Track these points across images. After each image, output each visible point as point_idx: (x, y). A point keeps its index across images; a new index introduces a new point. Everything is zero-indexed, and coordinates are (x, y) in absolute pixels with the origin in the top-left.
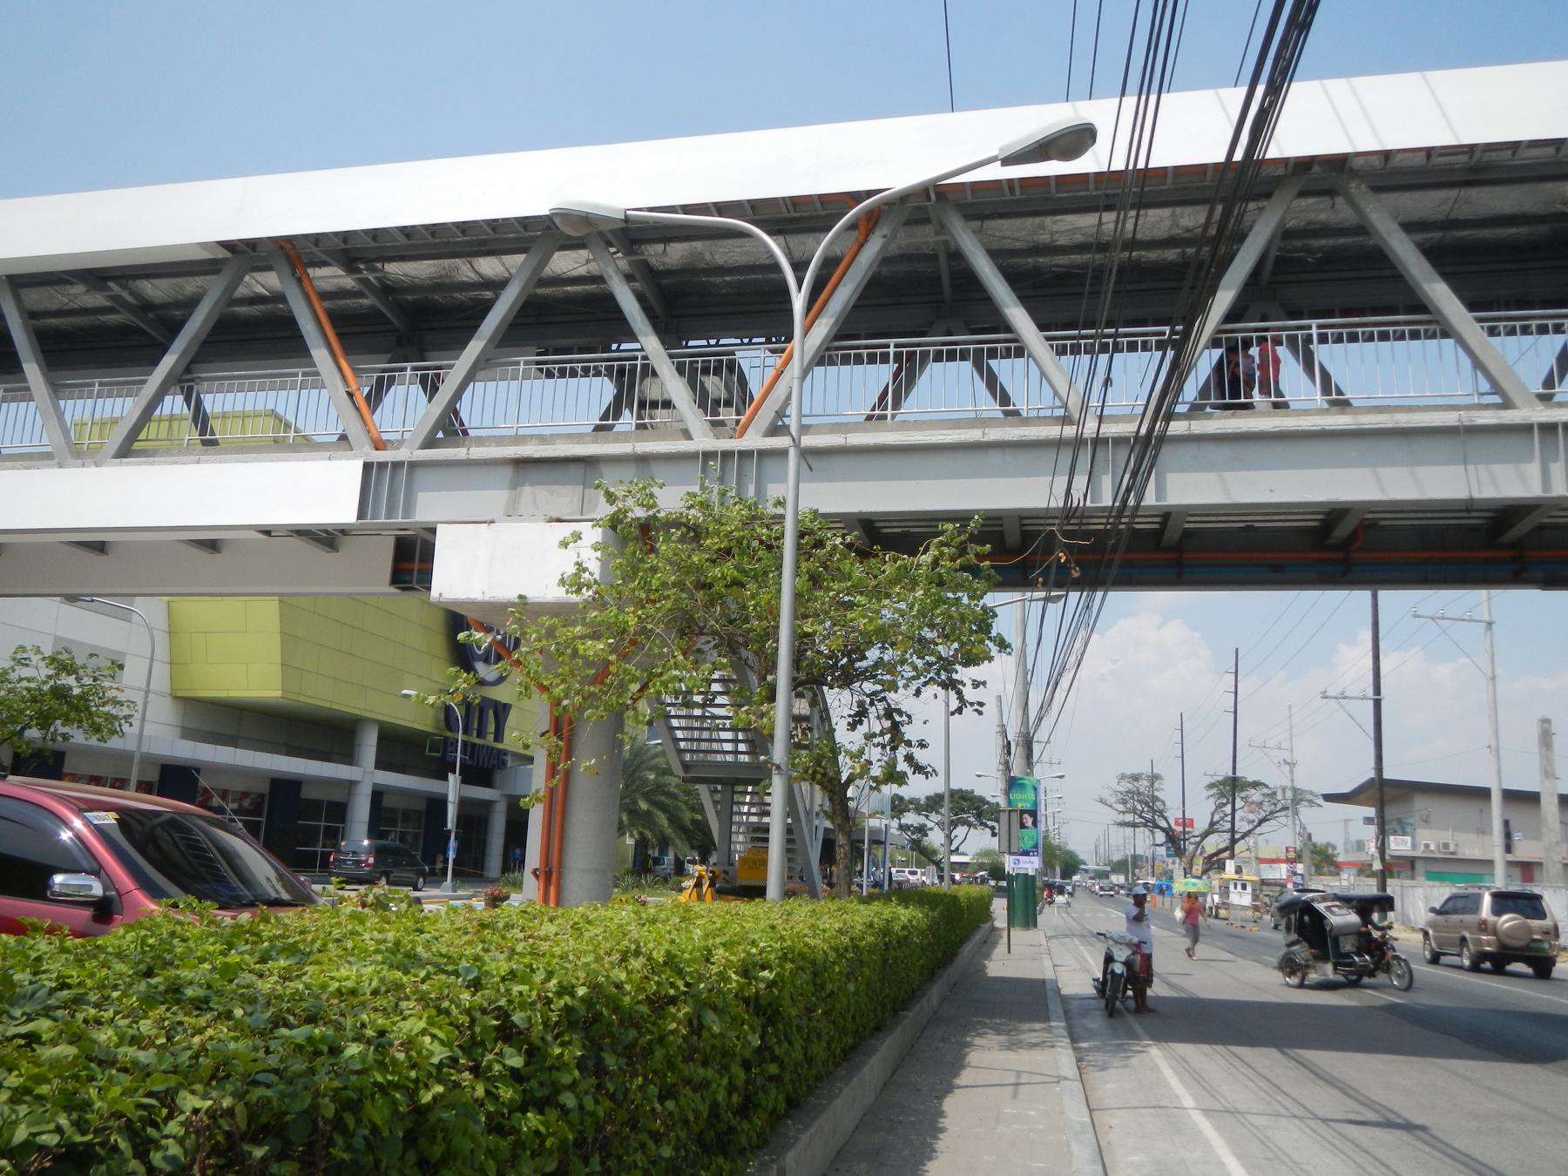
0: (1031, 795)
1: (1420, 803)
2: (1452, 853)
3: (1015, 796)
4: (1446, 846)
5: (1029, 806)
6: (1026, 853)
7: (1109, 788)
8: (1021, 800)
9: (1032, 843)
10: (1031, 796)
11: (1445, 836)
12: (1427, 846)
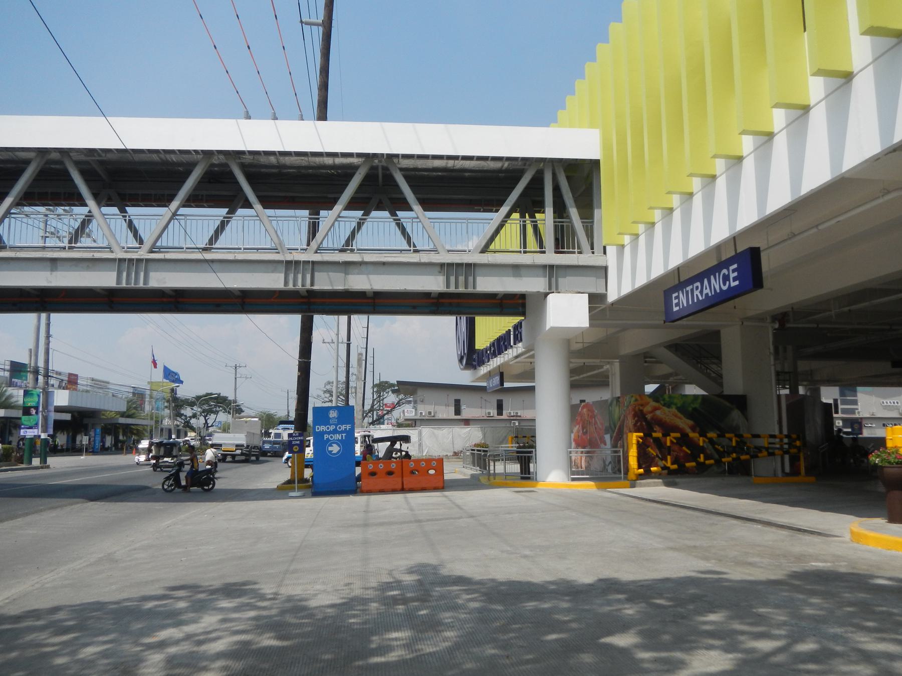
0: (36, 399)
1: (420, 393)
2: (434, 416)
3: (27, 400)
4: (430, 413)
5: (34, 404)
6: (31, 428)
7: (320, 389)
8: (30, 402)
9: (34, 422)
10: (36, 399)
11: (431, 408)
12: (421, 413)
